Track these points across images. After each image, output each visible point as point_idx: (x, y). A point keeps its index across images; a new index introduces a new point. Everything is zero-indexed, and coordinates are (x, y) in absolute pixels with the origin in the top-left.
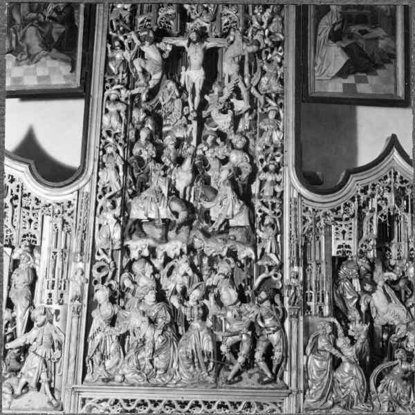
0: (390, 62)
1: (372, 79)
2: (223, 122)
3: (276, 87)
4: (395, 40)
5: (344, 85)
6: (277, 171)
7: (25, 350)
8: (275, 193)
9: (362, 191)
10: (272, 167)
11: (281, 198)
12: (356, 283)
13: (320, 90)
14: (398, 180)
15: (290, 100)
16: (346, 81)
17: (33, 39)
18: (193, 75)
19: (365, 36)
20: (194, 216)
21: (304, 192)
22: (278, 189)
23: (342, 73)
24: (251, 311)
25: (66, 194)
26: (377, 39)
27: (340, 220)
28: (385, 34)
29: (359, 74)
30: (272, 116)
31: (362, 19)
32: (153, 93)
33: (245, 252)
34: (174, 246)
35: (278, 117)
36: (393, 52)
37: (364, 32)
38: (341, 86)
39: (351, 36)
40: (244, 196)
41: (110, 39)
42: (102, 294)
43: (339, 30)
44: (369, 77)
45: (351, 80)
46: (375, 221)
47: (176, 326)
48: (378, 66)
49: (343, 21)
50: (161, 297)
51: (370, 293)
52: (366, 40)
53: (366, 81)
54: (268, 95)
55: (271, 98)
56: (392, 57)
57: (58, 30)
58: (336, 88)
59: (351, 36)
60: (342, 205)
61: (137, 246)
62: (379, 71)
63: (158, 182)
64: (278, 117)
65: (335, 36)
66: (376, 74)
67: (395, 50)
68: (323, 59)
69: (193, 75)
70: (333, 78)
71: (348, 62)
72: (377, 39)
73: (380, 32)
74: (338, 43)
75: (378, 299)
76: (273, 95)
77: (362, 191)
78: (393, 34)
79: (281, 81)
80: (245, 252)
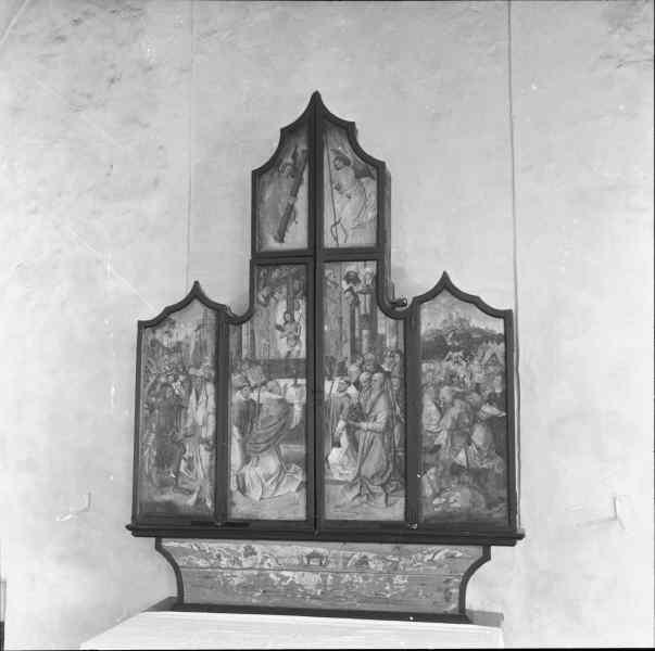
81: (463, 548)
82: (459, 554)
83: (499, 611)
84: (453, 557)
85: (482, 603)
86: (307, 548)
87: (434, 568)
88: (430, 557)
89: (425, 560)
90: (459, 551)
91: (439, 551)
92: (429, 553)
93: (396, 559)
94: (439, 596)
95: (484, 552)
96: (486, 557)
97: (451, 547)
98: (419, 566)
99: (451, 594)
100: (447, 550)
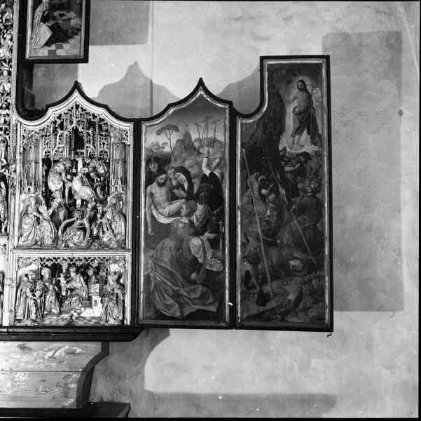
0: (77, 34)
1: (66, 46)
3: (8, 54)
4: (81, 19)
5: (49, 51)
6: (8, 108)
8: (5, 122)
9: (58, 118)
10: (4, 106)
11: (9, 125)
12: (63, 175)
13: (35, 55)
14: (80, 109)
15: (14, 62)
16: (49, 48)
19: (64, 18)
21: (21, 120)
22: (7, 119)
23: (48, 44)
26: (69, 19)
27: (46, 136)
28: (75, 15)
29: (58, 43)
30: (5, 73)
31: (61, 7)
35: (10, 73)
36: (79, 27)
37: (62, 15)
38: (47, 52)
39: (54, 18)
43: (47, 15)
44: (64, 45)
45: (53, 47)
46: (65, 136)
48: (71, 37)
49: (49, 10)
51: (71, 181)
52: (63, 20)
53: (58, 47)
54: (5, 61)
55: (5, 62)
56: (79, 30)
58: (44, 53)
59: (54, 18)
60: (46, 127)
62: (70, 41)
64: (10, 73)
66: (69, 43)
67: (81, 26)
68: (36, 35)
70: (42, 47)
71: (52, 35)
72: (69, 19)
73: (72, 14)
74: (47, 23)
75: (76, 185)
76: (7, 61)
77: (58, 118)
78: (80, 15)
79: (11, 51)
81: (83, 344)
82: (79, 350)
83: (127, 401)
84: (73, 353)
85: (112, 395)
87: (54, 365)
88: (50, 354)
89: (46, 357)
90: (79, 348)
91: (60, 348)
92: (50, 350)
93: (17, 357)
94: (57, 392)
95: (103, 349)
97: (72, 343)
98: (40, 363)
99: (69, 389)
100: (67, 347)
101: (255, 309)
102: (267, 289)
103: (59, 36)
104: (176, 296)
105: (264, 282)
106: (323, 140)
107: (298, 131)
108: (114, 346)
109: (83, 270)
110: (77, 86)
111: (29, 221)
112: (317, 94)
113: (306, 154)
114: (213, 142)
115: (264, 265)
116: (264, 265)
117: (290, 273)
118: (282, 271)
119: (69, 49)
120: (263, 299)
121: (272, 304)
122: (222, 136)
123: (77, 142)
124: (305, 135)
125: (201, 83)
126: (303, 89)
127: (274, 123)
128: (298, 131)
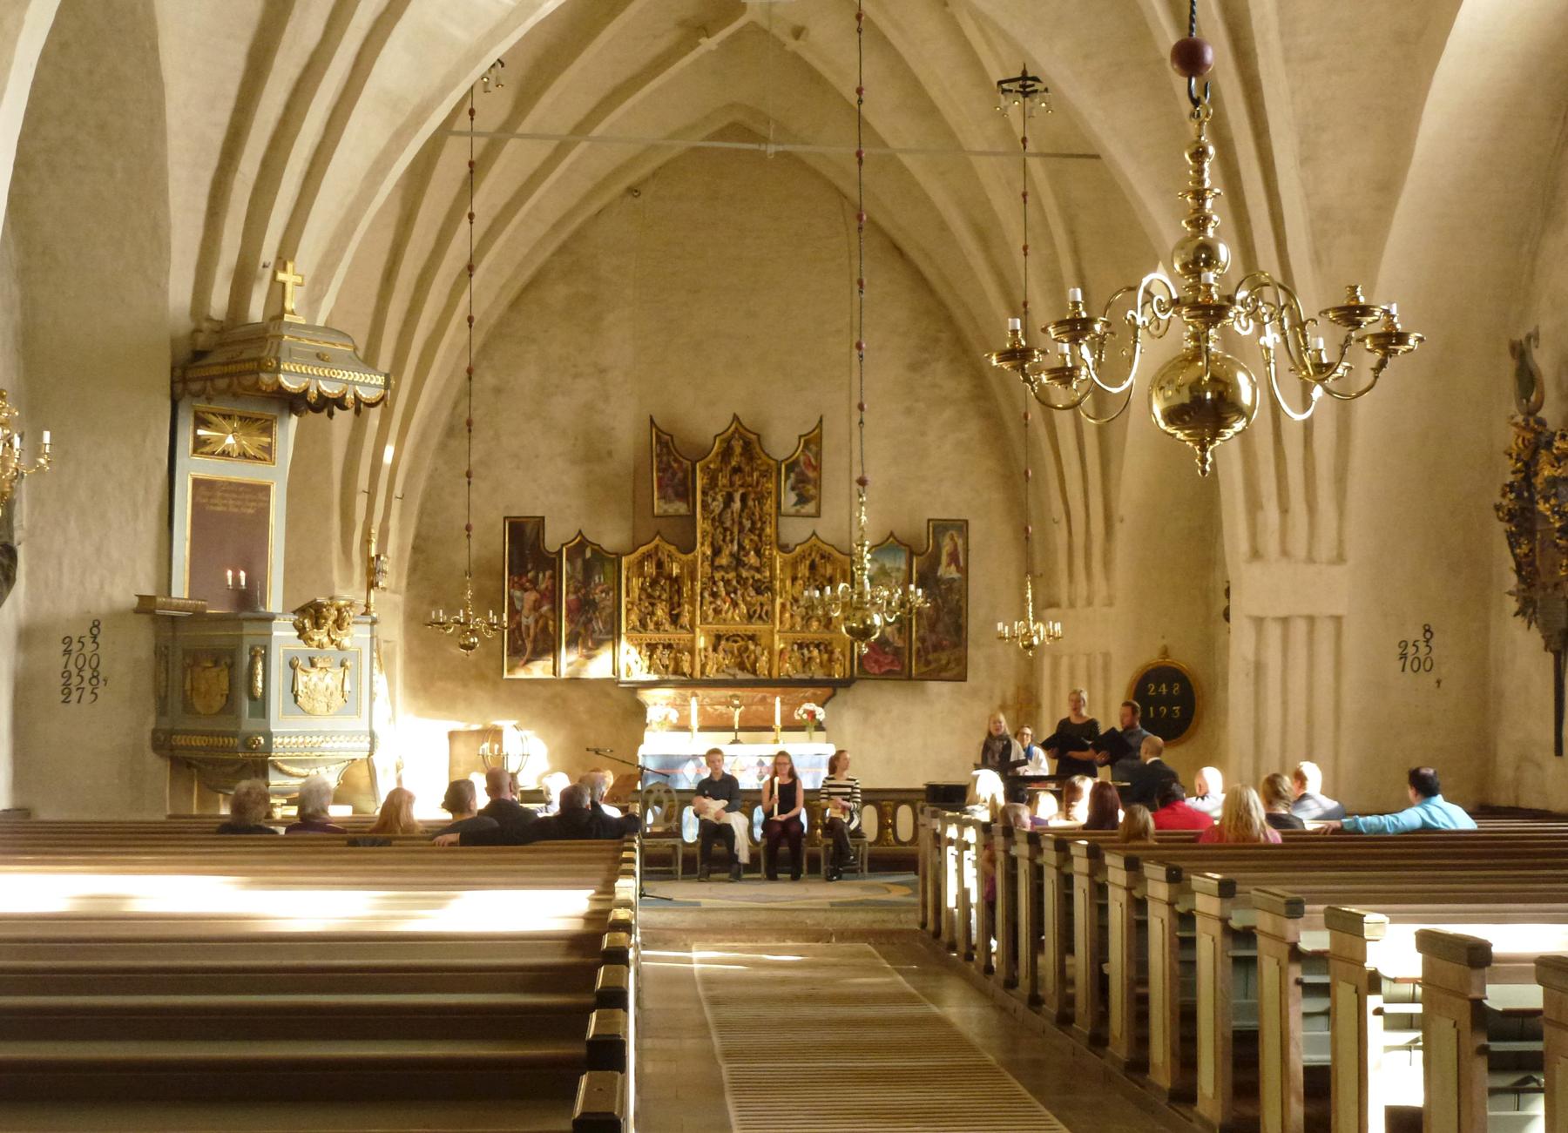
2: (748, 524)
7: (678, 615)
17: (670, 491)
18: (737, 505)
20: (738, 562)
24: (760, 598)
25: (690, 556)
31: (803, 482)
32: (720, 515)
33: (758, 576)
34: (731, 575)
40: (758, 553)
41: (704, 493)
42: (706, 594)
47: (735, 604)
50: (728, 594)
57: (681, 489)
58: (793, 510)
61: (718, 576)
63: (726, 552)
65: (793, 489)
69: (737, 505)
80: (758, 576)
86: (730, 692)
96: (833, 695)
101: (924, 669)
102: (931, 657)
103: (803, 500)
104: (876, 661)
105: (927, 653)
106: (964, 571)
107: (949, 565)
108: (840, 692)
109: (817, 646)
110: (814, 534)
111: (787, 615)
112: (960, 542)
113: (953, 580)
114: (898, 570)
115: (929, 644)
116: (929, 644)
117: (943, 649)
118: (937, 647)
119: (810, 508)
120: (928, 663)
121: (933, 666)
122: (904, 567)
123: (813, 567)
124: (953, 567)
125: (892, 534)
126: (952, 539)
127: (935, 561)
128: (949, 565)
